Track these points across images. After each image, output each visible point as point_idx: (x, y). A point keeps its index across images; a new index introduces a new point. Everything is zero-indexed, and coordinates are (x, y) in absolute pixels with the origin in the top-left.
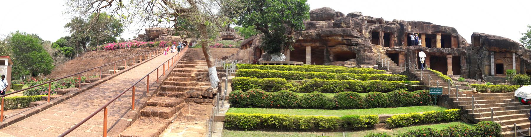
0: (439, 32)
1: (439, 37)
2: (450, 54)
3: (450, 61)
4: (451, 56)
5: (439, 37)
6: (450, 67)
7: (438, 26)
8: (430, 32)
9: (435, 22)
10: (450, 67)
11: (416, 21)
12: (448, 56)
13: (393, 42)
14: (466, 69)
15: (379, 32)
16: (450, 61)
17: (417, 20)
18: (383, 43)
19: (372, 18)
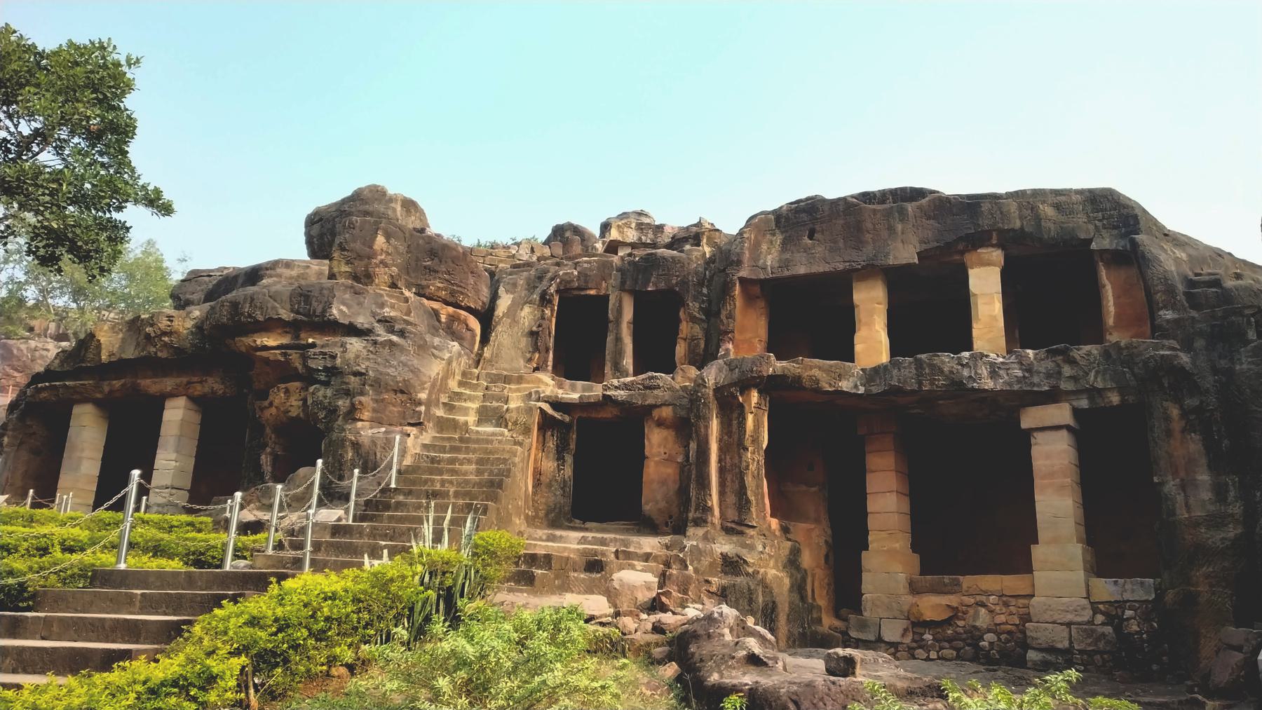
0: (978, 240)
1: (985, 284)
2: (1052, 397)
3: (1053, 456)
4: (1061, 413)
5: (985, 284)
6: (1056, 505)
7: (971, 205)
8: (905, 253)
9: (955, 179)
10: (1056, 505)
11: (831, 194)
12: (1030, 418)
13: (681, 349)
14: (1216, 521)
15: (606, 298)
16: (1053, 456)
17: (837, 185)
18: (628, 362)
19: (660, 228)
